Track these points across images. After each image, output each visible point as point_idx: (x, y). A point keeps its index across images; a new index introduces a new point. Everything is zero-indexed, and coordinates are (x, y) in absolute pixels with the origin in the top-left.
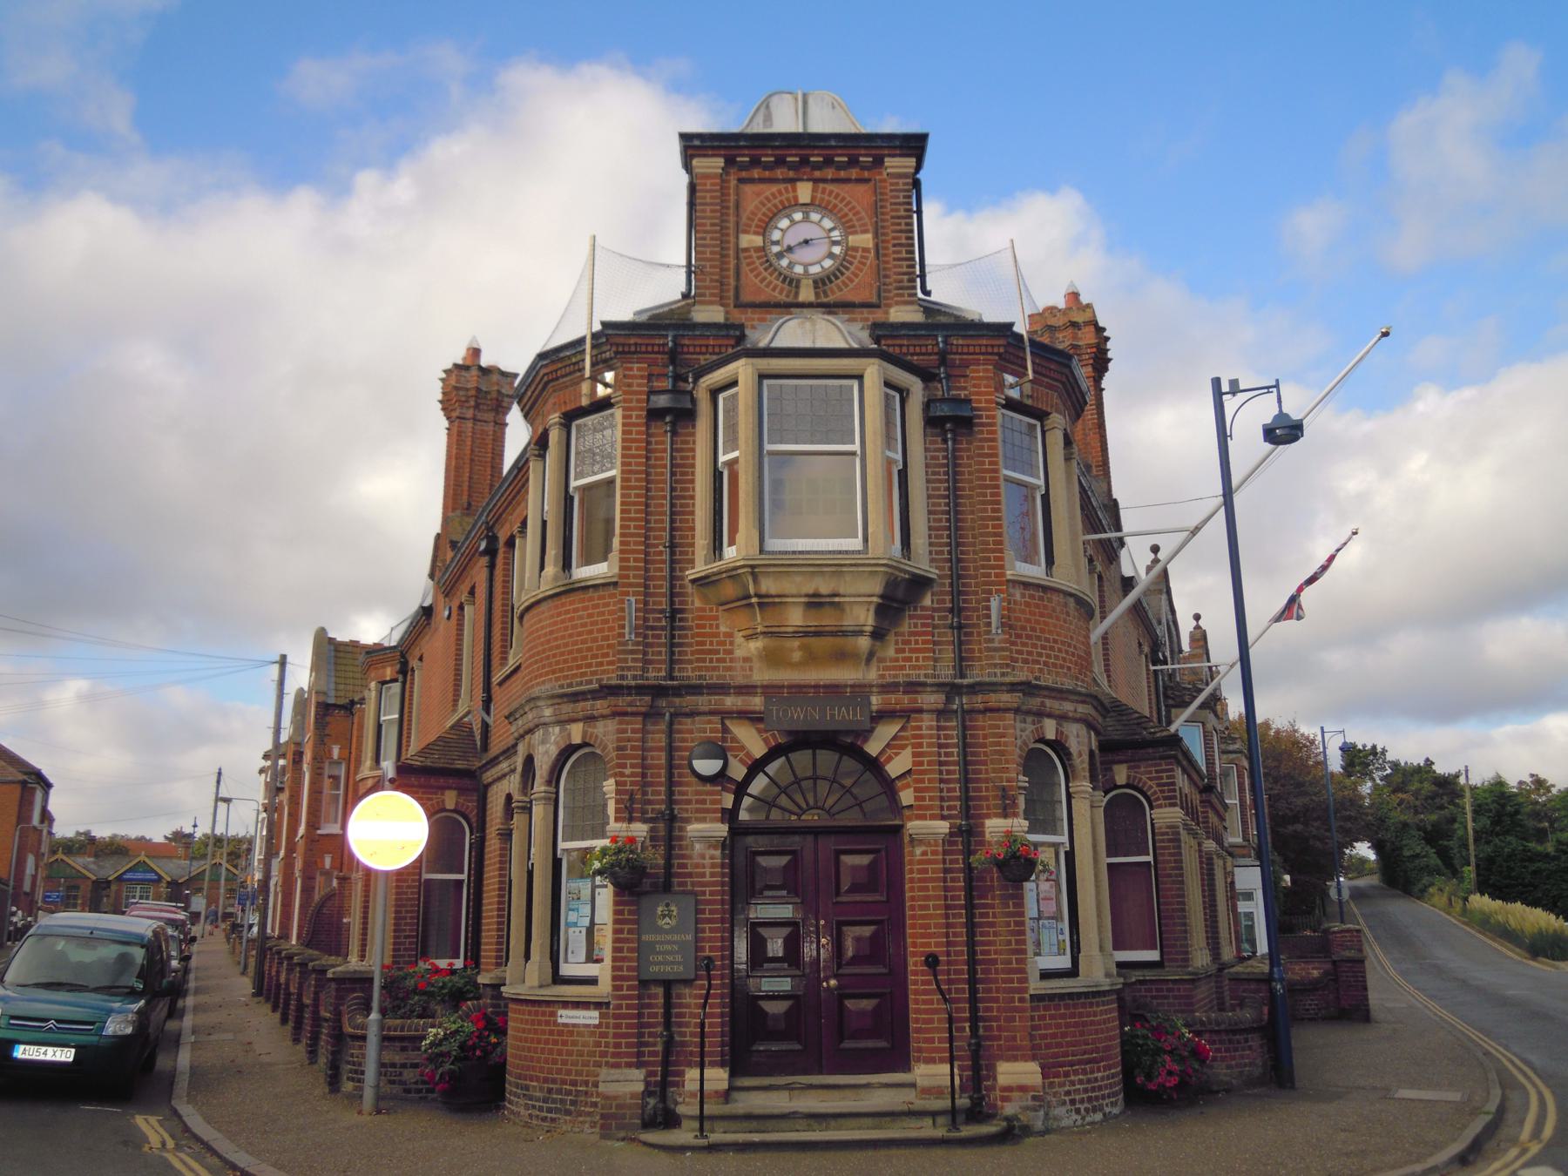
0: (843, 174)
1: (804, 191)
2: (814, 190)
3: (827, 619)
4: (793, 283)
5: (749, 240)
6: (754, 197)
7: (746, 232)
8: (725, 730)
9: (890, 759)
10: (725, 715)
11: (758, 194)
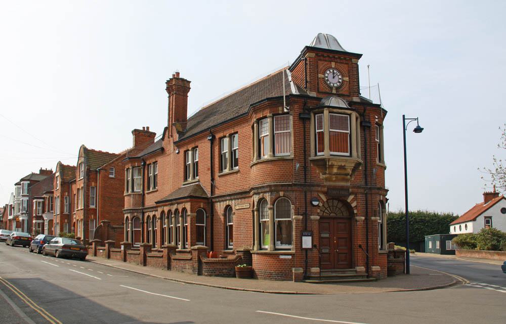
0: (341, 61)
1: (333, 65)
2: (335, 65)
3: (342, 172)
4: (331, 88)
5: (320, 76)
6: (322, 65)
7: (320, 74)
8: (318, 195)
9: (352, 203)
10: (318, 191)
11: (323, 64)
